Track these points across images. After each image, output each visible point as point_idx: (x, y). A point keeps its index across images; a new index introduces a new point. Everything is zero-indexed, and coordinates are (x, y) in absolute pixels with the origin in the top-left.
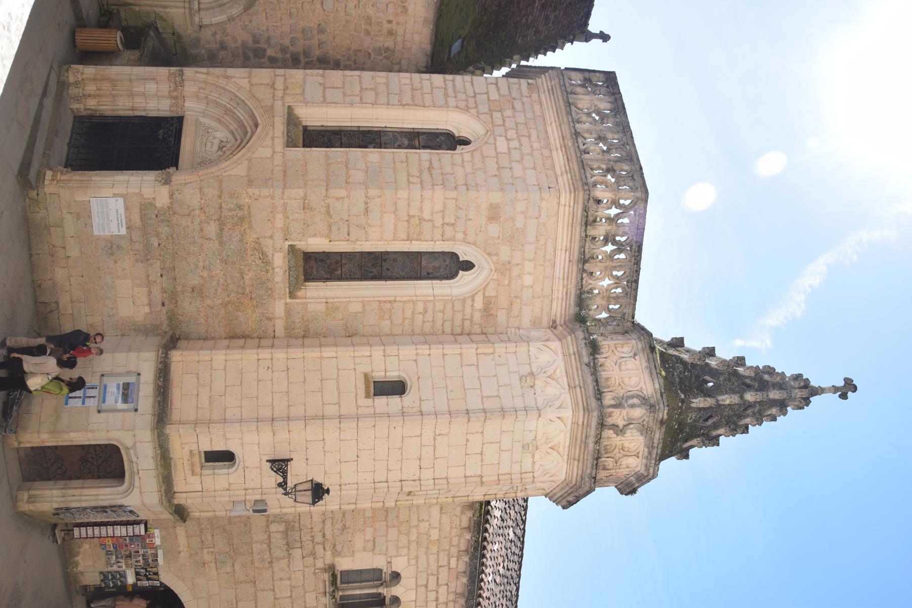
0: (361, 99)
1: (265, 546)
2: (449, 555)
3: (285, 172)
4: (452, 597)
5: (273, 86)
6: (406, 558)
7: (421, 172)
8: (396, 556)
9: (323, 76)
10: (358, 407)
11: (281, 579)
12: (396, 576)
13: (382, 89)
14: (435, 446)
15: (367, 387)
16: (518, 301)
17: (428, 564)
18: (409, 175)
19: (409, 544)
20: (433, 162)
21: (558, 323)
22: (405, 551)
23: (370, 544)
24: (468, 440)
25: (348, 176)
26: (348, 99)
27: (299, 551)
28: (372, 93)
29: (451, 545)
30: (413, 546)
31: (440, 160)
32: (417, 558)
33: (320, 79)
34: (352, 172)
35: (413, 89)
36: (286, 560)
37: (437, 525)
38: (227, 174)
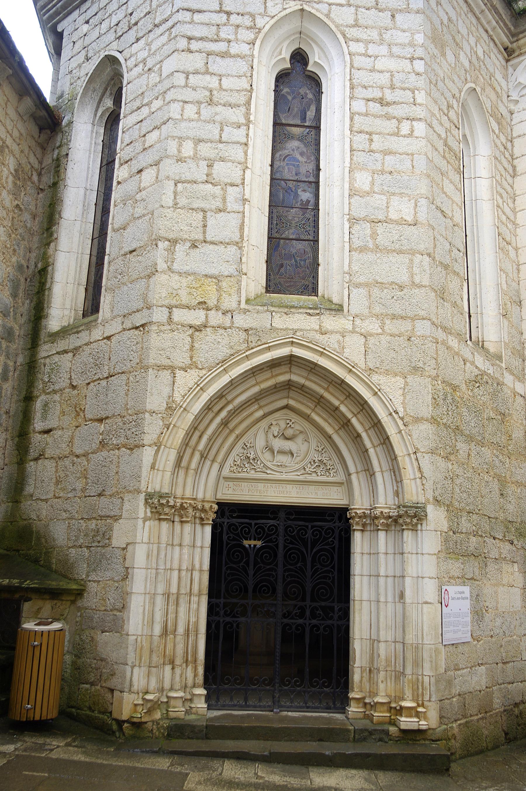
0: (232, 185)
3: (394, 317)
5: (198, 329)
7: (388, 117)
9: (174, 242)
13: (205, 150)
16: (493, 79)
18: (397, 134)
20: (370, 96)
21: (510, 46)
25: (401, 222)
26: (231, 205)
28: (218, 167)
31: (365, 87)
33: (180, 249)
34: (393, 216)
35: (211, 102)
38: (401, 410)
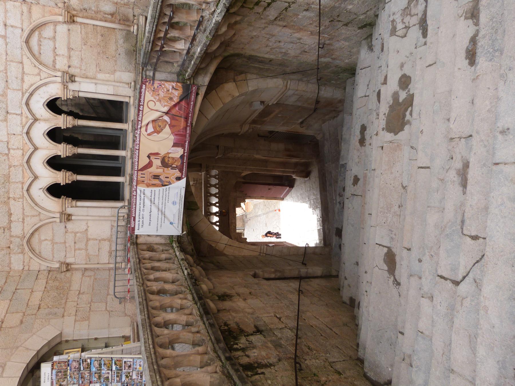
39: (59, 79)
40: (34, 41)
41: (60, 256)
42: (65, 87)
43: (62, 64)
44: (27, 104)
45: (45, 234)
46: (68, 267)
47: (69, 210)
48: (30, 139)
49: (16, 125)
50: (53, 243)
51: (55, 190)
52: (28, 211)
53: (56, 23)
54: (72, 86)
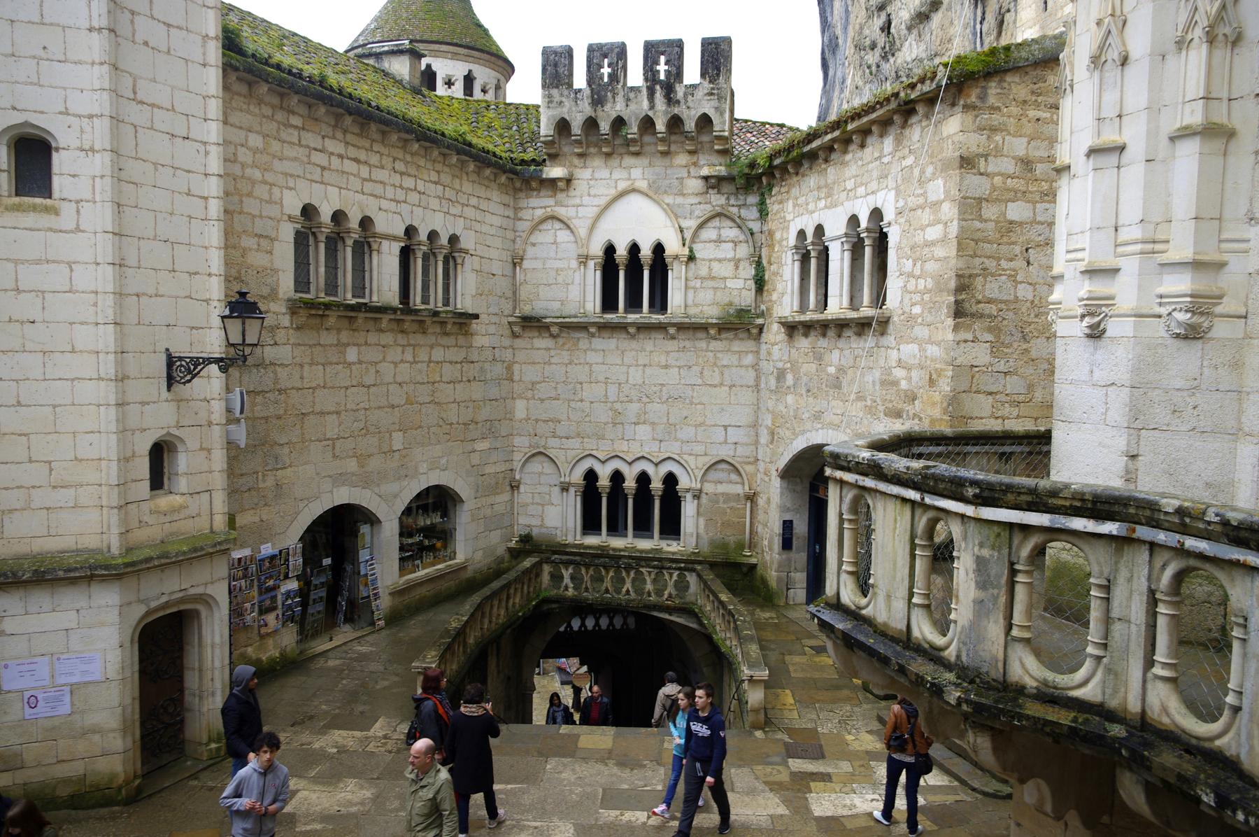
1: (259, 399)
2: (284, 125)
4: (339, 135)
6: (285, 191)
8: (282, 206)
10: (78, 229)
11: (302, 378)
12: (308, 211)
14: (153, 105)
15: (34, 208)
17: (295, 159)
19: (265, 183)
22: (276, 190)
23: (264, 242)
24: (146, 43)
27: (267, 349)
29: (272, 118)
30: (269, 177)
32: (286, 174)
36: (279, 369)
37: (243, 133)
39: (693, 485)
40: (724, 466)
41: (526, 479)
42: (688, 490)
43: (709, 488)
44: (669, 458)
45: (548, 468)
46: (514, 487)
47: (572, 490)
48: (638, 459)
49: (651, 449)
50: (540, 474)
51: (591, 476)
52: (571, 454)
53: (743, 484)
54: (689, 496)
